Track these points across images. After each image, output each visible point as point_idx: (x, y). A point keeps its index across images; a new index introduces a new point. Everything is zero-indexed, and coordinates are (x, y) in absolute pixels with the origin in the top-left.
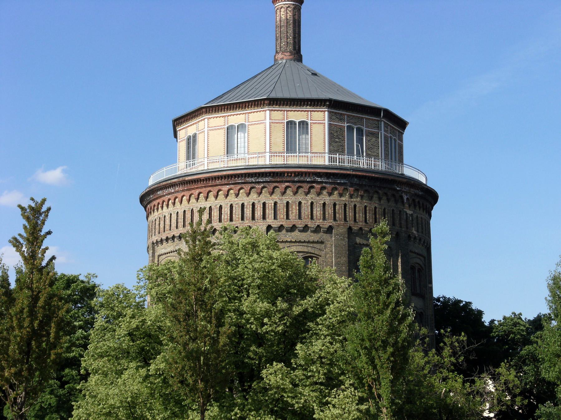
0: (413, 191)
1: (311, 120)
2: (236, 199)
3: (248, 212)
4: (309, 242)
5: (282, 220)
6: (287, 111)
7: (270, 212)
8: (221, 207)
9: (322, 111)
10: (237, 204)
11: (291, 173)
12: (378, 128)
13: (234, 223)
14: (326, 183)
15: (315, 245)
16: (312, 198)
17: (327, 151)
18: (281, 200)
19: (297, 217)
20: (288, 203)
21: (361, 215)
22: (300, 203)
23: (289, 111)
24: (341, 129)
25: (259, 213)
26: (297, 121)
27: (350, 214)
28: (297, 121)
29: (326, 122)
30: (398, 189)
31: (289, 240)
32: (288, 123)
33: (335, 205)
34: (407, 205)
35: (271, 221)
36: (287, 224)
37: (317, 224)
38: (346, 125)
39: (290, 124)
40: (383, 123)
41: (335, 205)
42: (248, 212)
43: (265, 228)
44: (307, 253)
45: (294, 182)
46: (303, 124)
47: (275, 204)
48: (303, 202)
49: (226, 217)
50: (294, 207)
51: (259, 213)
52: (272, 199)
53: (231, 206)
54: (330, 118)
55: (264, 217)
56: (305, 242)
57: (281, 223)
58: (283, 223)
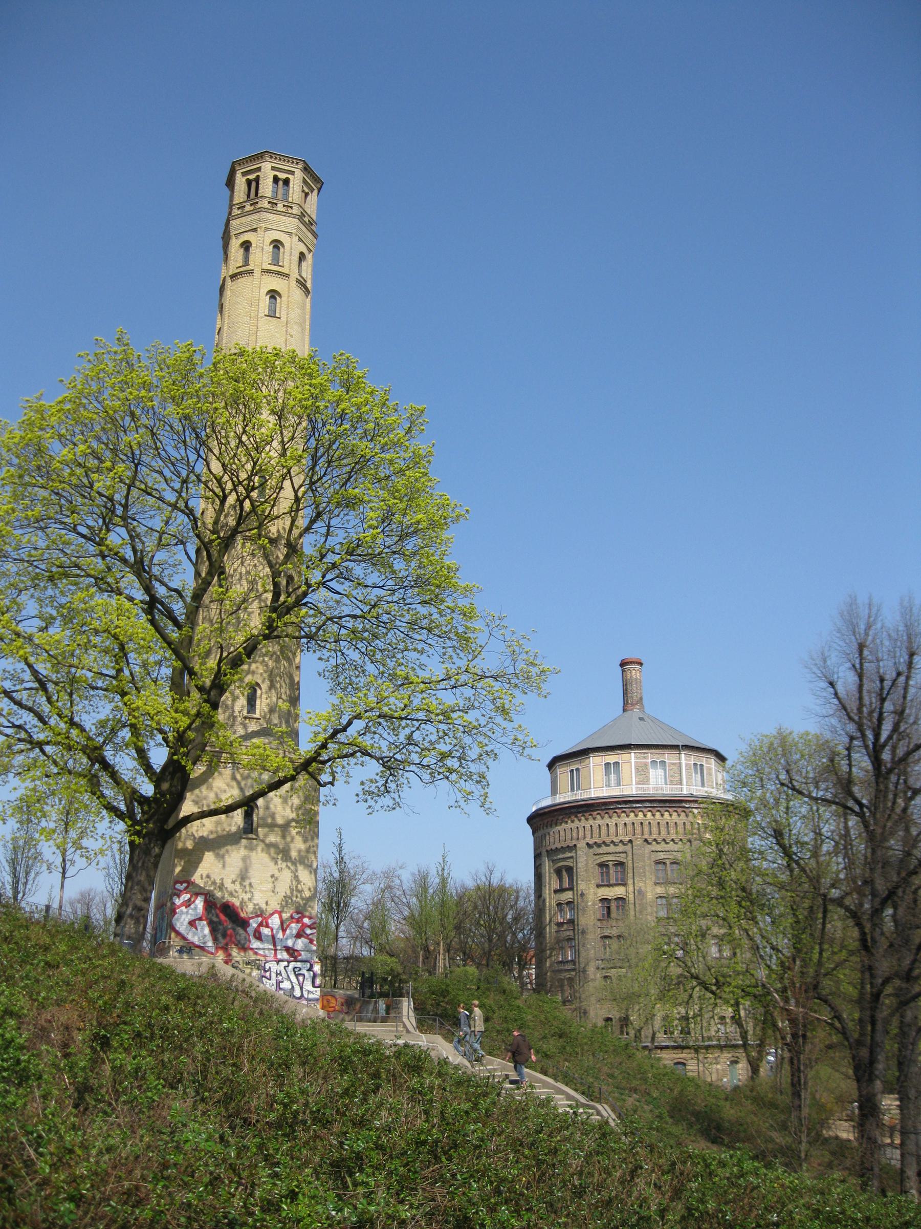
3: (575, 835)
7: (588, 833)
12: (680, 759)
17: (634, 783)
24: (646, 764)
25: (581, 834)
27: (646, 829)
29: (633, 761)
33: (633, 824)
36: (599, 841)
40: (683, 755)
41: (633, 824)
42: (575, 835)
45: (602, 810)
46: (617, 763)
51: (581, 834)
54: (636, 758)
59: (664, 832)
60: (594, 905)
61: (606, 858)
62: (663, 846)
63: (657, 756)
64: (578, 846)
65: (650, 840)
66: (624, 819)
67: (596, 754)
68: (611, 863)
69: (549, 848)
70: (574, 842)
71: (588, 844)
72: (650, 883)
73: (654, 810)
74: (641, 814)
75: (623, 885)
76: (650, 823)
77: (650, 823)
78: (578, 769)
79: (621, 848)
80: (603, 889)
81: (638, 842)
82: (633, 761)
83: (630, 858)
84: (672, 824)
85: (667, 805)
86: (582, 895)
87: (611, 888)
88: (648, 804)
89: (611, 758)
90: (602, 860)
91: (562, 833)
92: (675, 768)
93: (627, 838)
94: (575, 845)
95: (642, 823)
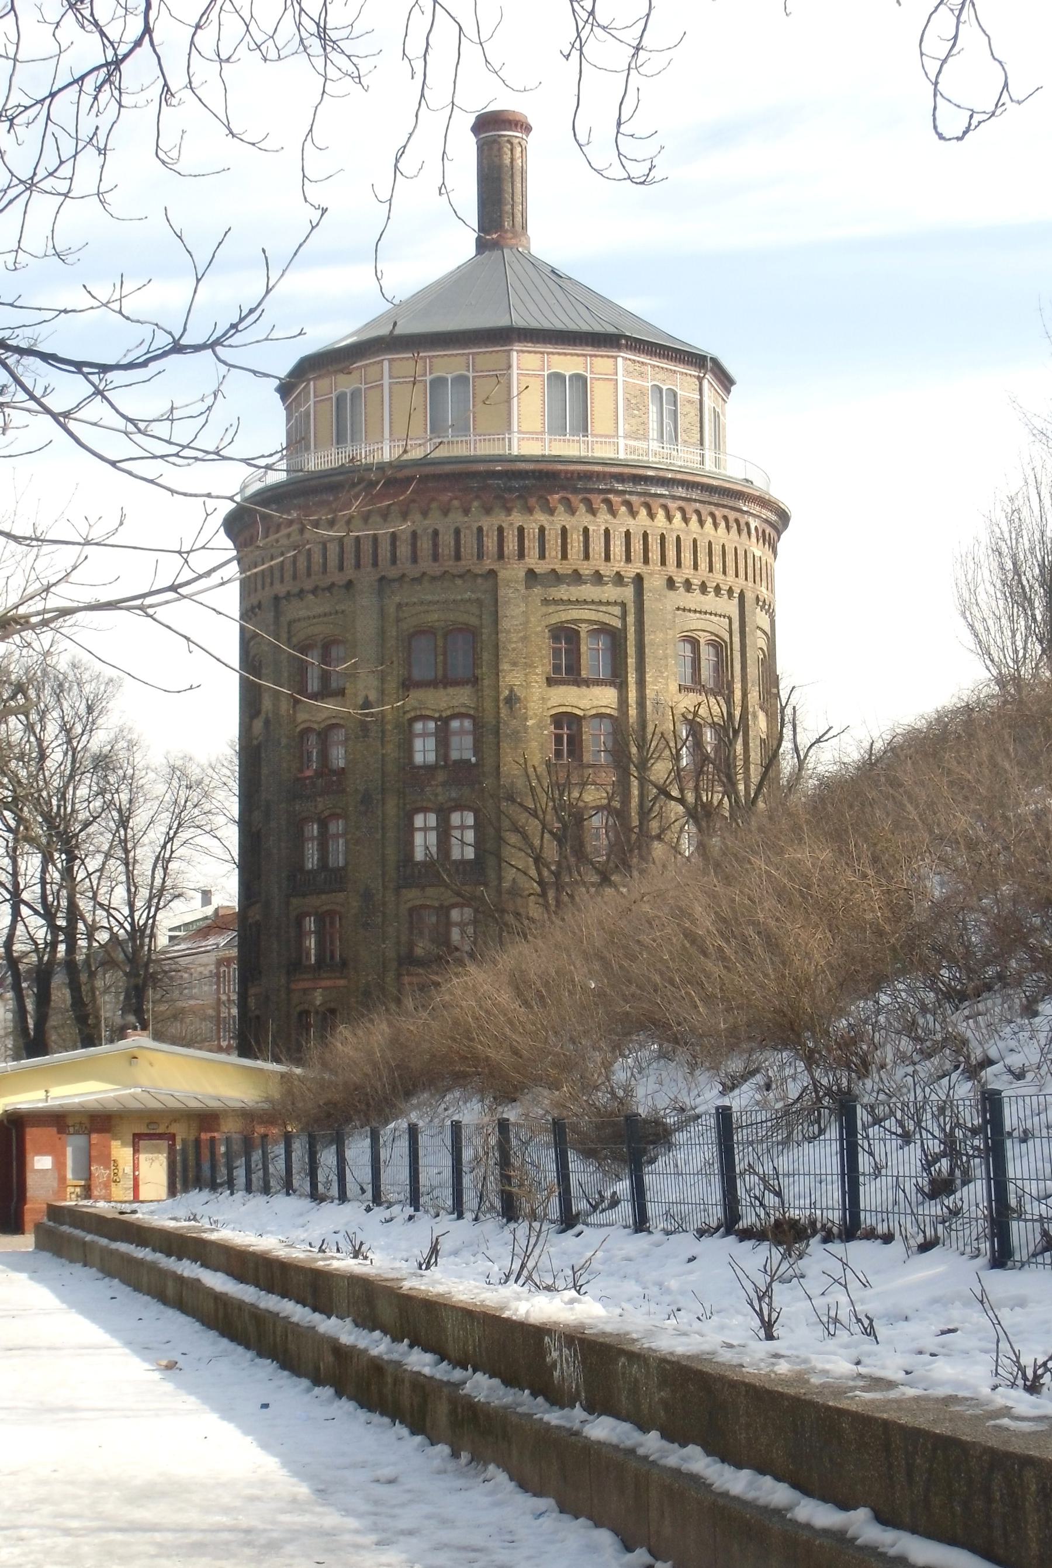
0: (766, 514)
1: (592, 372)
2: (466, 519)
3: (490, 544)
4: (600, 603)
5: (553, 562)
6: (548, 353)
8: (436, 533)
9: (612, 357)
10: (467, 528)
11: (572, 472)
13: (463, 562)
14: (631, 493)
15: (610, 609)
16: (606, 521)
18: (552, 523)
19: (582, 556)
20: (564, 531)
21: (687, 555)
22: (586, 530)
23: (552, 353)
26: (567, 374)
27: (671, 554)
28: (567, 374)
30: (745, 509)
31: (565, 598)
32: (549, 376)
33: (645, 535)
34: (754, 539)
35: (532, 561)
37: (615, 569)
38: (650, 384)
39: (557, 378)
41: (645, 535)
42: (490, 544)
43: (522, 574)
44: (595, 622)
45: (575, 491)
46: (580, 380)
47: (542, 530)
48: (591, 528)
49: (447, 552)
50: (575, 536)
51: (511, 545)
52: (535, 521)
53: (457, 532)
54: (628, 373)
55: (521, 555)
56: (593, 602)
57: (552, 567)
58: (556, 567)
59: (703, 565)
60: (540, 726)
61: (575, 614)
62: (694, 600)
63: (662, 375)
64: (502, 574)
65: (679, 580)
66: (623, 522)
67: (530, 346)
68: (584, 628)
69: (393, 573)
70: (488, 564)
71: (531, 573)
72: (673, 687)
73: (689, 508)
74: (661, 514)
75: (612, 684)
76: (678, 538)
77: (678, 538)
78: (461, 381)
79: (610, 592)
80: (563, 689)
81: (654, 582)
82: (620, 378)
83: (631, 619)
84: (717, 549)
85: (715, 499)
86: (512, 700)
87: (584, 689)
88: (681, 492)
89: (568, 363)
90: (565, 616)
91: (447, 539)
92: (694, 412)
93: (630, 571)
94: (492, 574)
95: (663, 537)
